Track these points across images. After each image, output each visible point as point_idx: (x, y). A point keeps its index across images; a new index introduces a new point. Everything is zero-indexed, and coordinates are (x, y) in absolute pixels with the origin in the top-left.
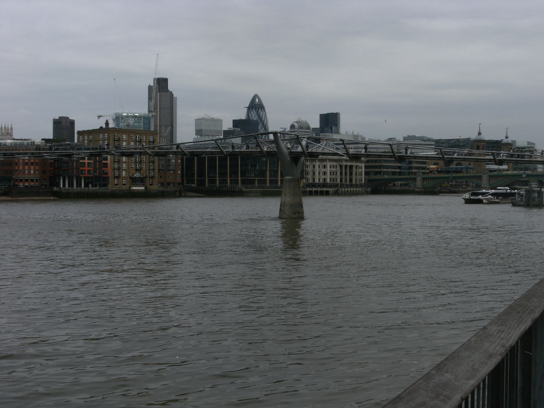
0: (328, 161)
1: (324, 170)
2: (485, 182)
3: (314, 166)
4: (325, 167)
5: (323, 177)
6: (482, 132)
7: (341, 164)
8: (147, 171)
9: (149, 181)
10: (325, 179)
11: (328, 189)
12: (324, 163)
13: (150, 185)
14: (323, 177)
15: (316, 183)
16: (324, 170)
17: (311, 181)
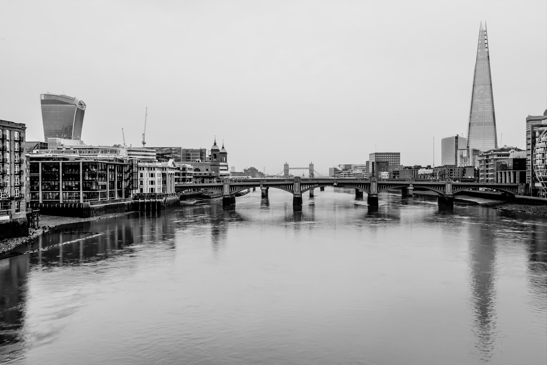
0: (156, 169)
1: (151, 179)
2: (297, 190)
3: (142, 176)
4: (152, 175)
5: (151, 186)
6: (216, 142)
7: (164, 172)
8: (13, 188)
9: (14, 204)
10: (152, 189)
11: (160, 200)
12: (152, 172)
13: (17, 211)
14: (151, 186)
15: (145, 194)
16: (151, 179)
17: (138, 191)
